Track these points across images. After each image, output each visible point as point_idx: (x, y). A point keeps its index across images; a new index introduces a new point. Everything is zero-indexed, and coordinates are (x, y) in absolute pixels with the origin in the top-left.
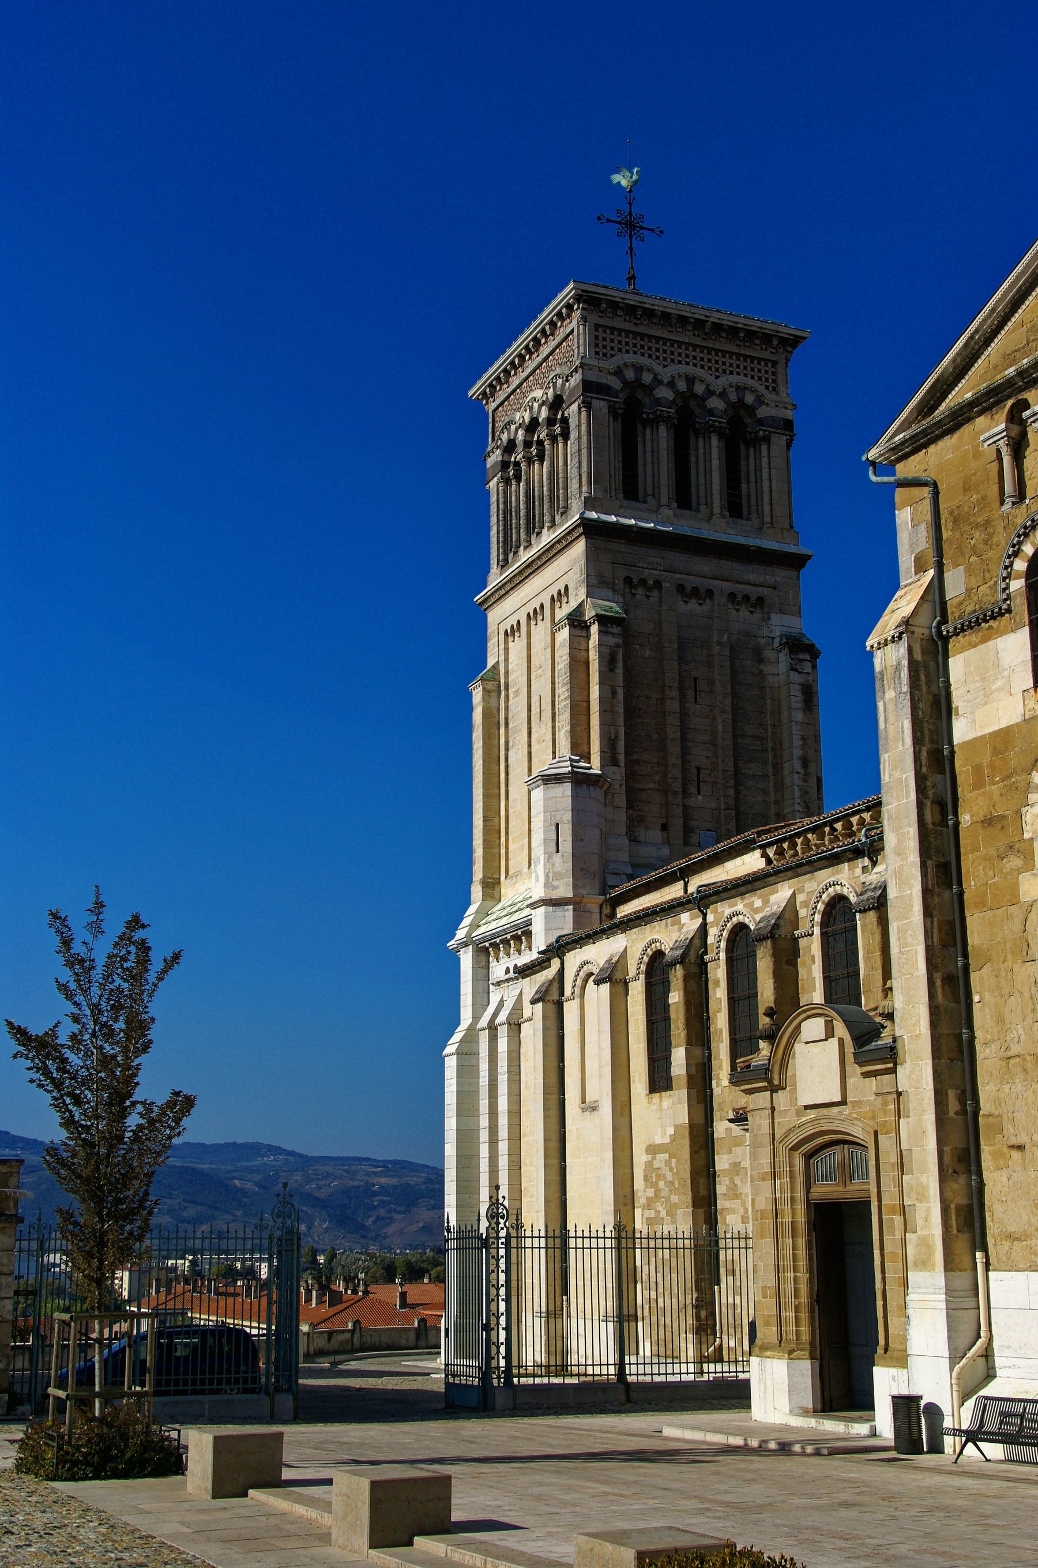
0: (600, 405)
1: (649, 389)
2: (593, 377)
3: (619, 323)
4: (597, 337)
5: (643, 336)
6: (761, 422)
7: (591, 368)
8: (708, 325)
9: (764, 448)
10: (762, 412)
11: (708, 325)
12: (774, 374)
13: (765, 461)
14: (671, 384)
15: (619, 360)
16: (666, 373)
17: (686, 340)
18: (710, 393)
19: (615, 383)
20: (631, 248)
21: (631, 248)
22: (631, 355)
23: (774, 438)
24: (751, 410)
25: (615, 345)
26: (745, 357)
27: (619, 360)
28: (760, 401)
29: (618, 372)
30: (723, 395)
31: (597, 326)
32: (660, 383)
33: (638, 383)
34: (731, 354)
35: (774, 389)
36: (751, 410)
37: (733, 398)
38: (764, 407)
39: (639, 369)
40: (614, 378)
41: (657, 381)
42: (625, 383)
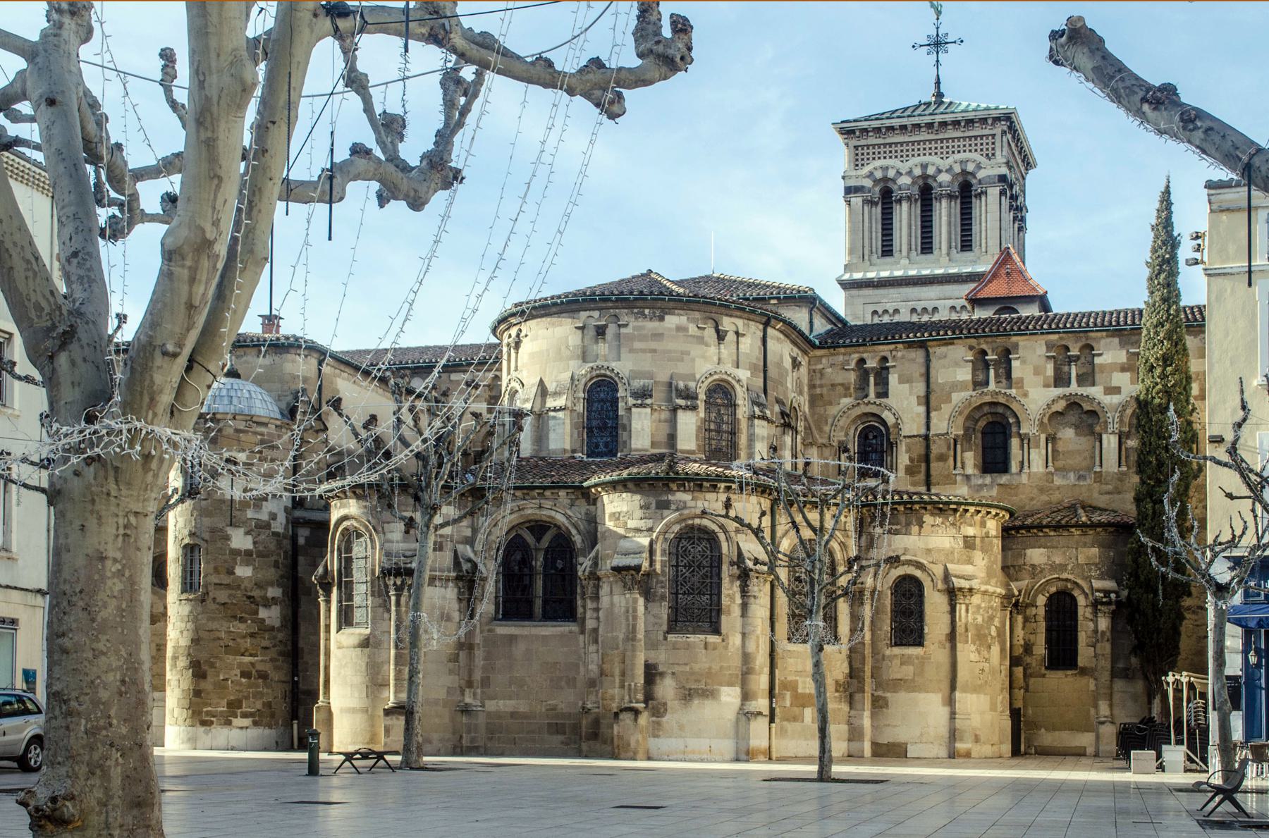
0: (857, 201)
1: (894, 181)
2: (852, 183)
3: (872, 140)
4: (857, 155)
5: (890, 145)
6: (980, 182)
7: (850, 177)
8: (936, 125)
9: (983, 198)
10: (981, 175)
11: (936, 125)
12: (993, 143)
13: (983, 208)
14: (910, 173)
15: (866, 170)
16: (904, 167)
17: (922, 138)
18: (940, 171)
19: (868, 183)
20: (938, 61)
21: (938, 61)
22: (882, 160)
23: (990, 191)
24: (973, 174)
25: (871, 156)
26: (970, 138)
27: (866, 170)
28: (979, 167)
29: (870, 175)
30: (949, 170)
31: (856, 147)
32: (901, 174)
33: (885, 179)
34: (959, 139)
35: (993, 154)
36: (973, 174)
37: (957, 169)
38: (983, 170)
39: (886, 169)
40: (867, 179)
41: (899, 173)
42: (876, 182)
